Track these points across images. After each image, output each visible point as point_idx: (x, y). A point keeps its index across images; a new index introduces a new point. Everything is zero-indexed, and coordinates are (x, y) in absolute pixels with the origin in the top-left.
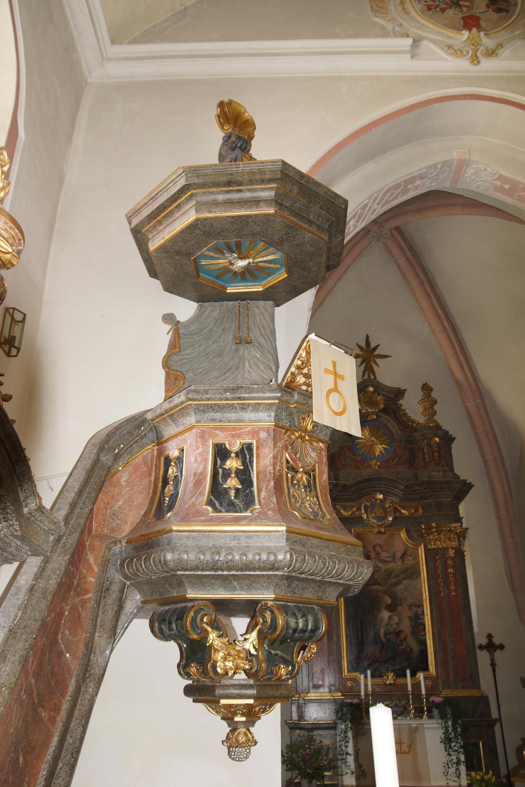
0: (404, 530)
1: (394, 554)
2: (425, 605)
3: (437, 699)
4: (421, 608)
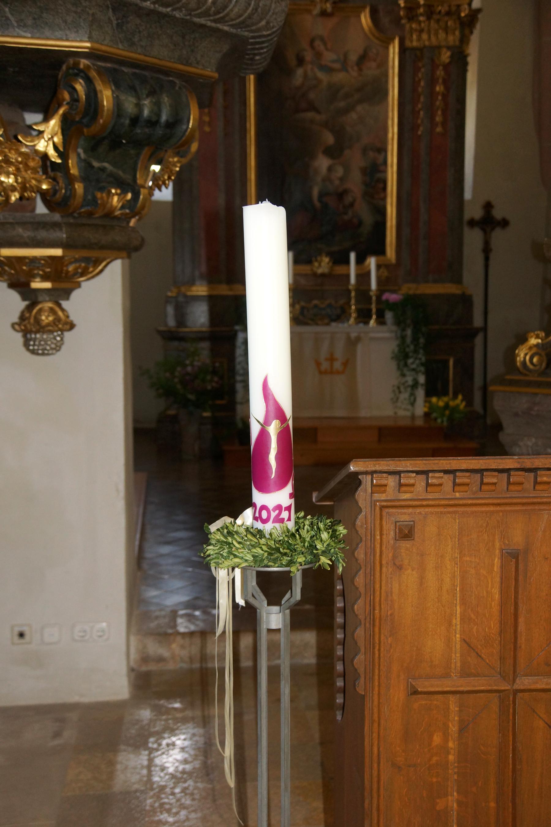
0: (368, 10)
1: (346, 55)
2: (390, 147)
4: (383, 154)
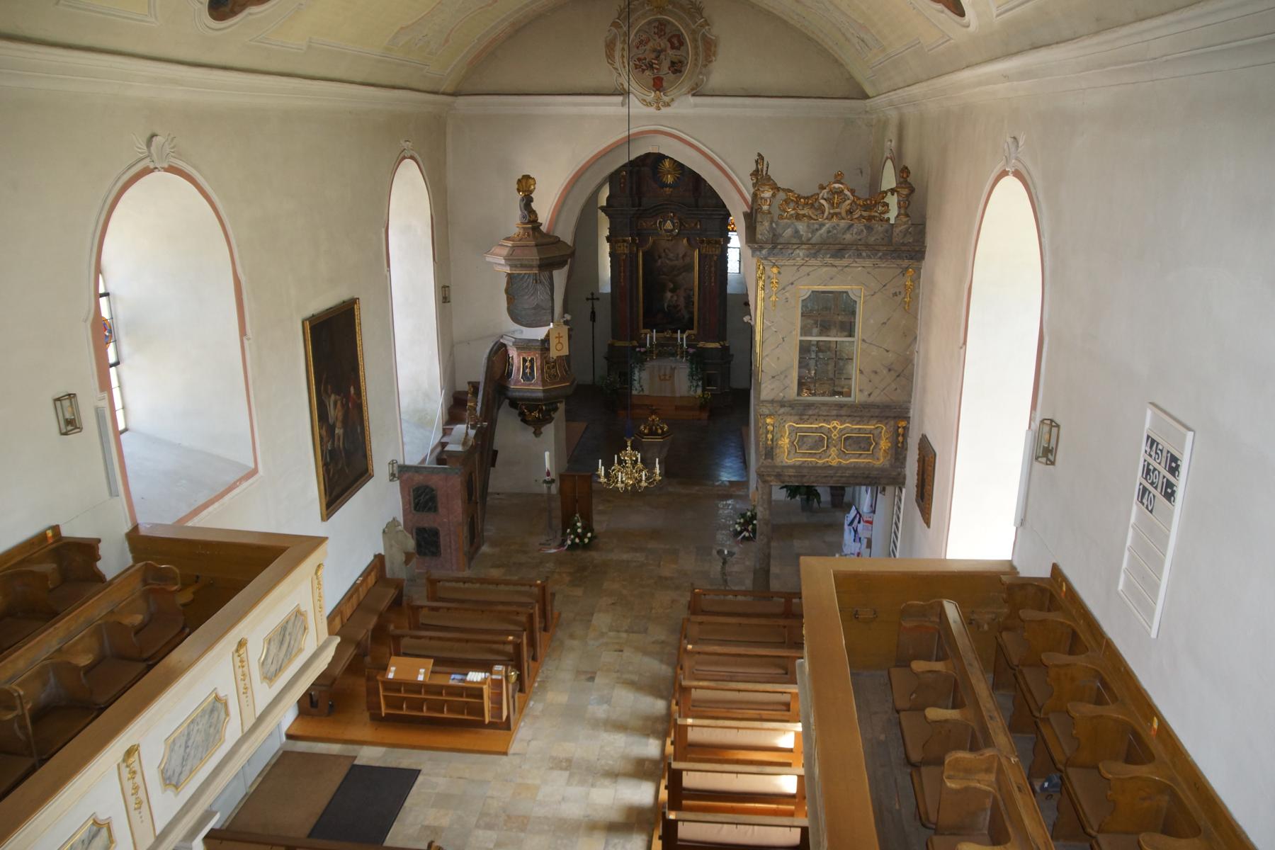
3: (691, 351)
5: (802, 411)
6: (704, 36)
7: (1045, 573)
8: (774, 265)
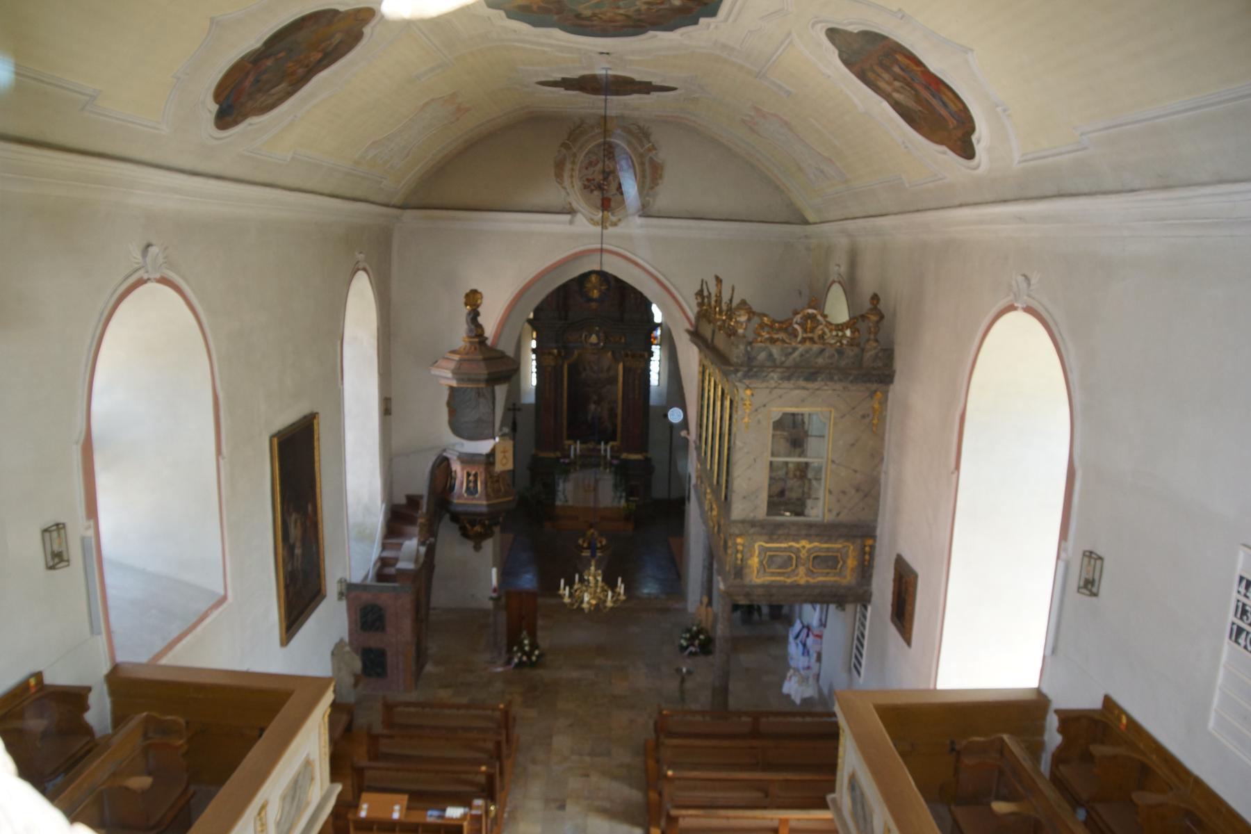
3: (615, 462)
5: (771, 531)
6: (651, 160)
7: (1095, 703)
8: (748, 387)
